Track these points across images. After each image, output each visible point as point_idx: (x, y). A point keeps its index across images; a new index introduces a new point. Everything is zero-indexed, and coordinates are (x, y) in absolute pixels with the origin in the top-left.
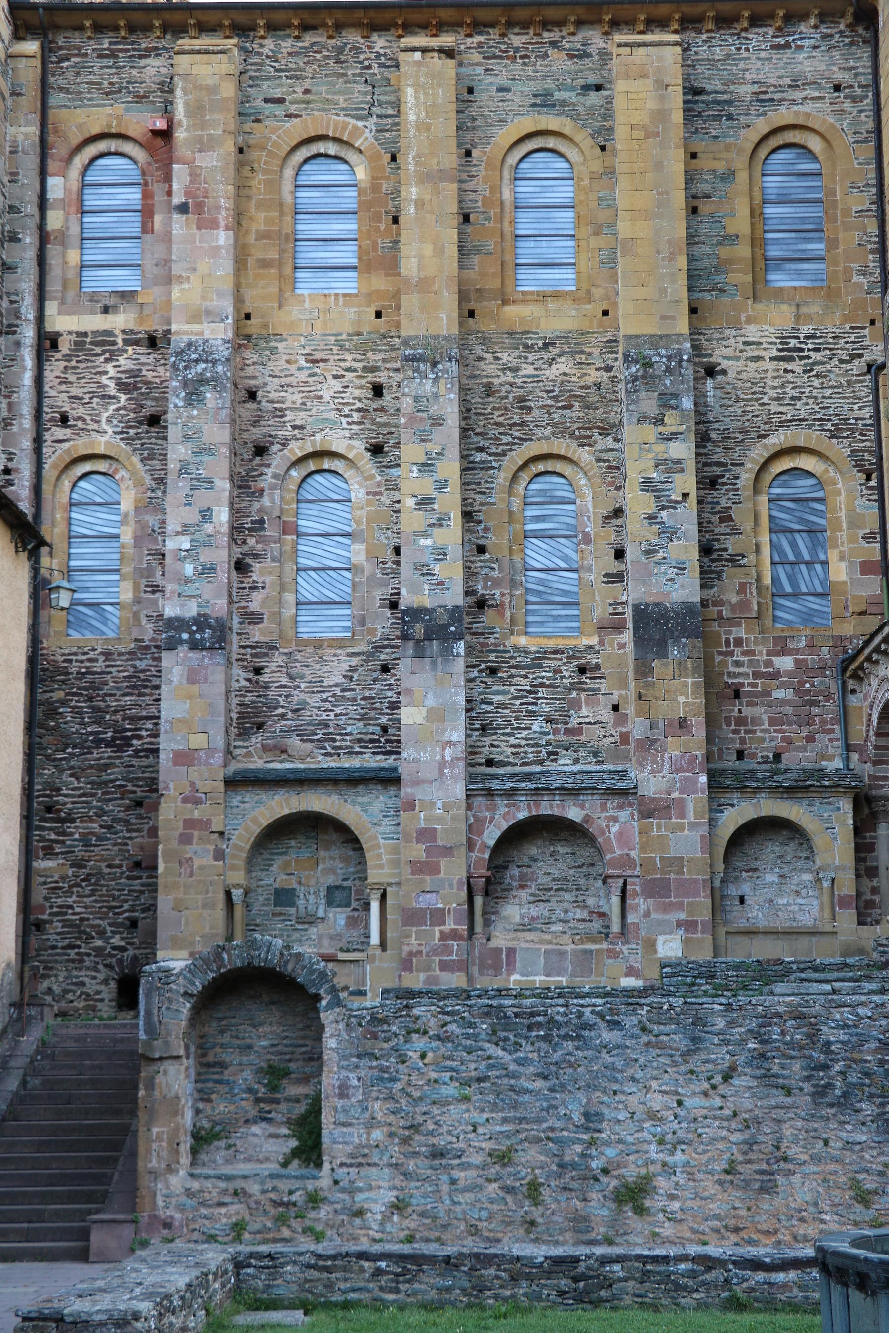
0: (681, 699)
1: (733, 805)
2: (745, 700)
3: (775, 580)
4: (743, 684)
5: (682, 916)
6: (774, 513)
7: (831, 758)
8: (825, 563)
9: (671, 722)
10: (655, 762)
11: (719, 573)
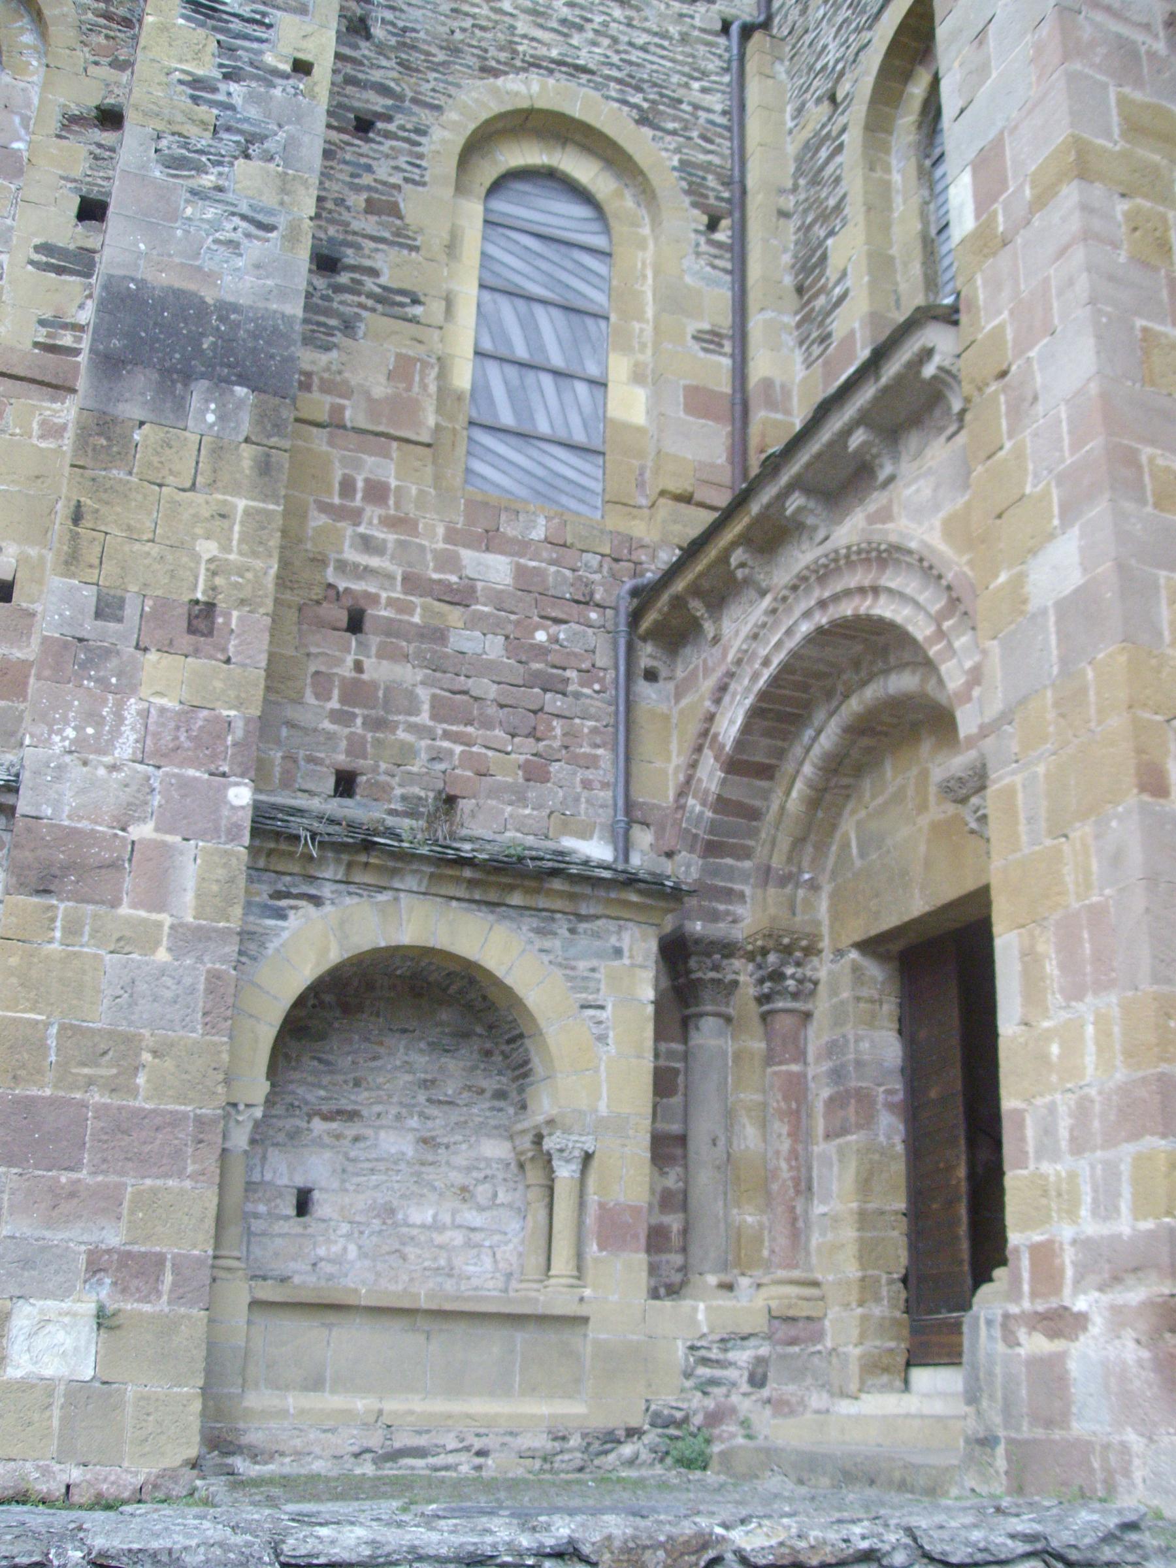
0: (208, 548)
1: (317, 901)
2: (374, 641)
3: (480, 388)
4: (374, 599)
5: (113, 1237)
6: (492, 250)
7: (585, 833)
8: (599, 384)
9: (163, 604)
10: (92, 716)
11: (348, 327)
